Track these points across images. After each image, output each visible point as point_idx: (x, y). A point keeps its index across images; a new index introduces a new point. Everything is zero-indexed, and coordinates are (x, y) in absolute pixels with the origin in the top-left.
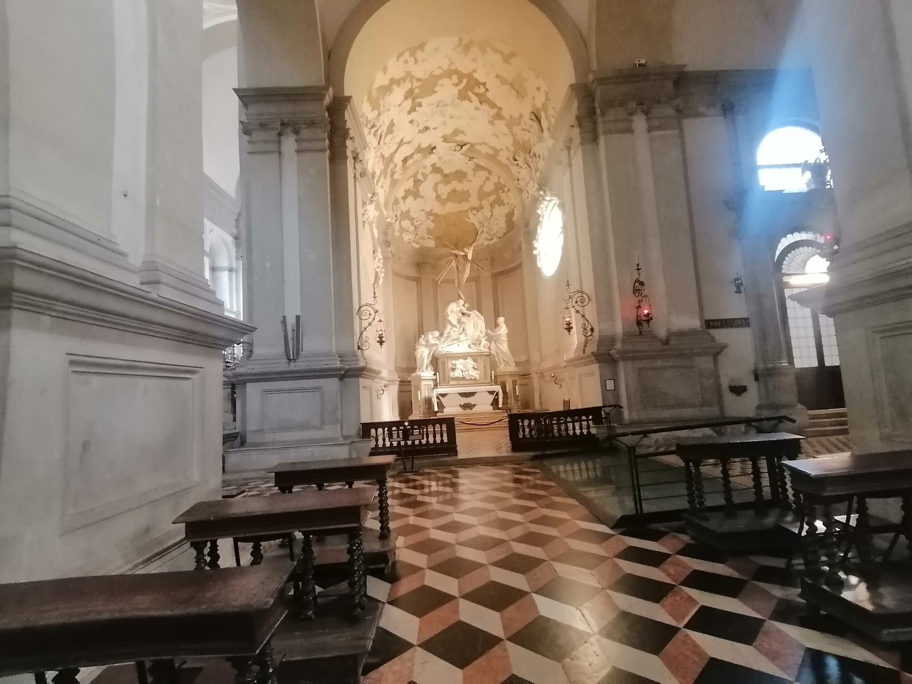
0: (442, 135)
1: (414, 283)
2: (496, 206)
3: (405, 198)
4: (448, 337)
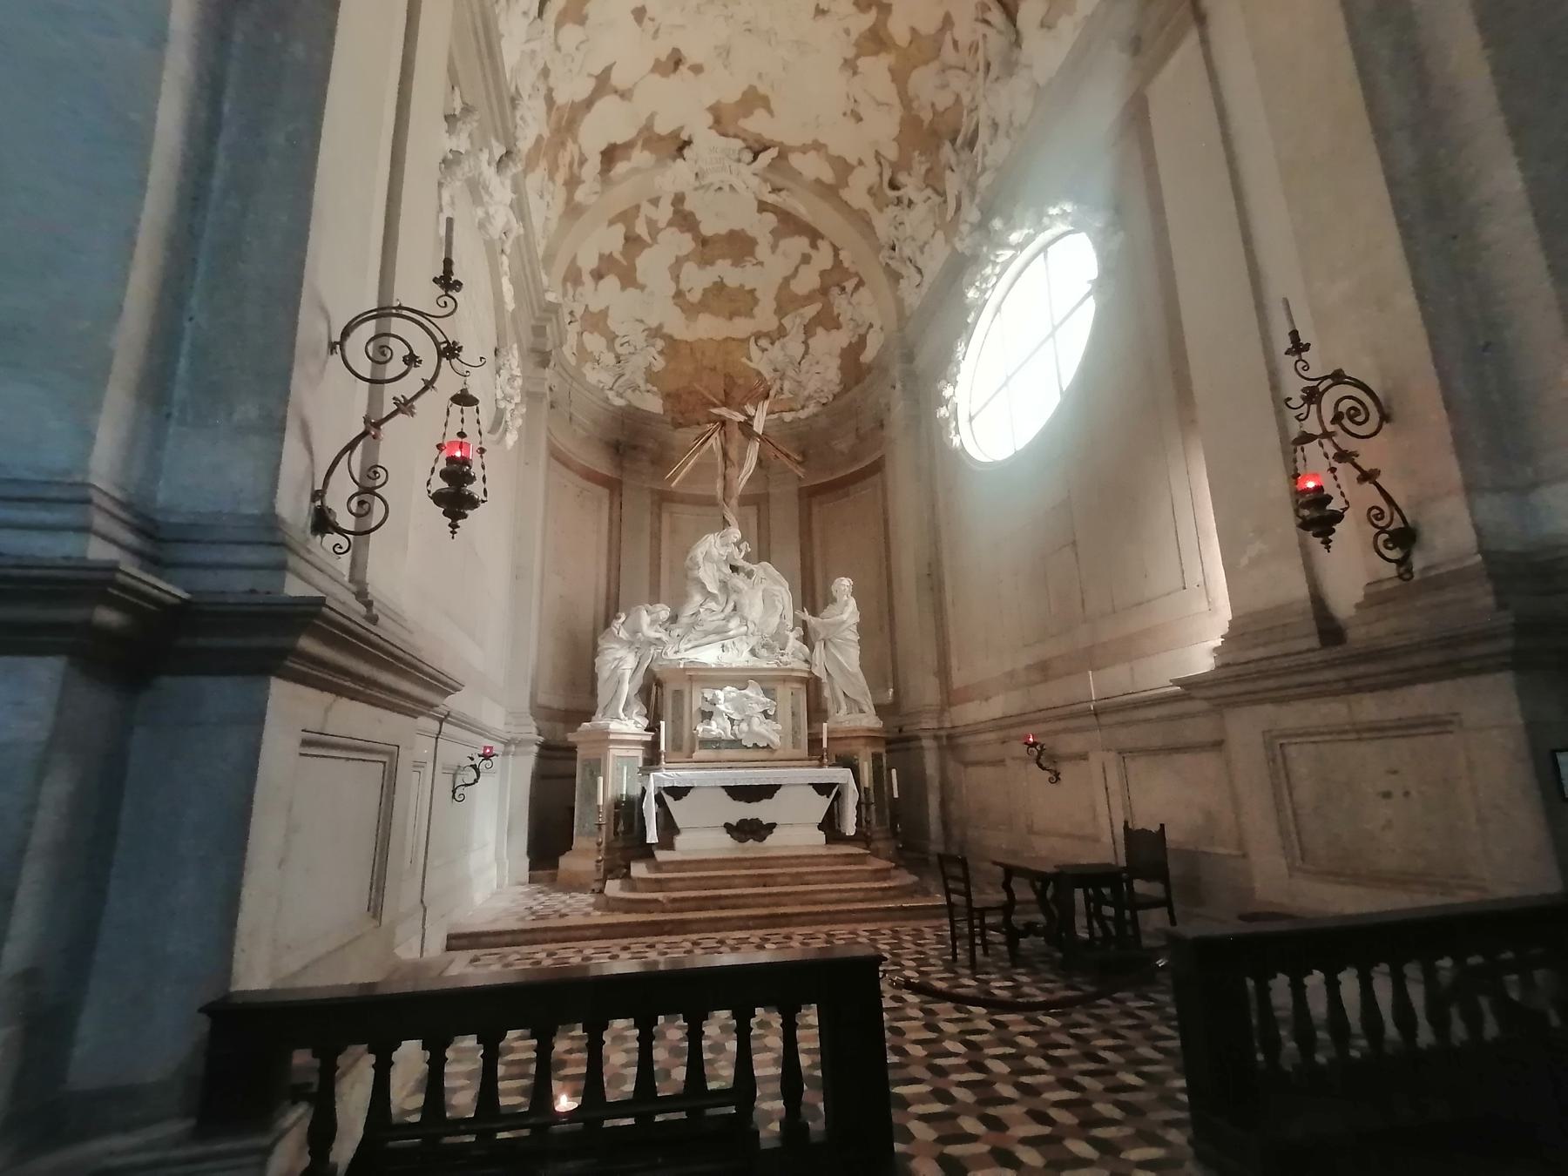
1: (603, 492)
2: (820, 331)
3: (598, 275)
4: (692, 626)
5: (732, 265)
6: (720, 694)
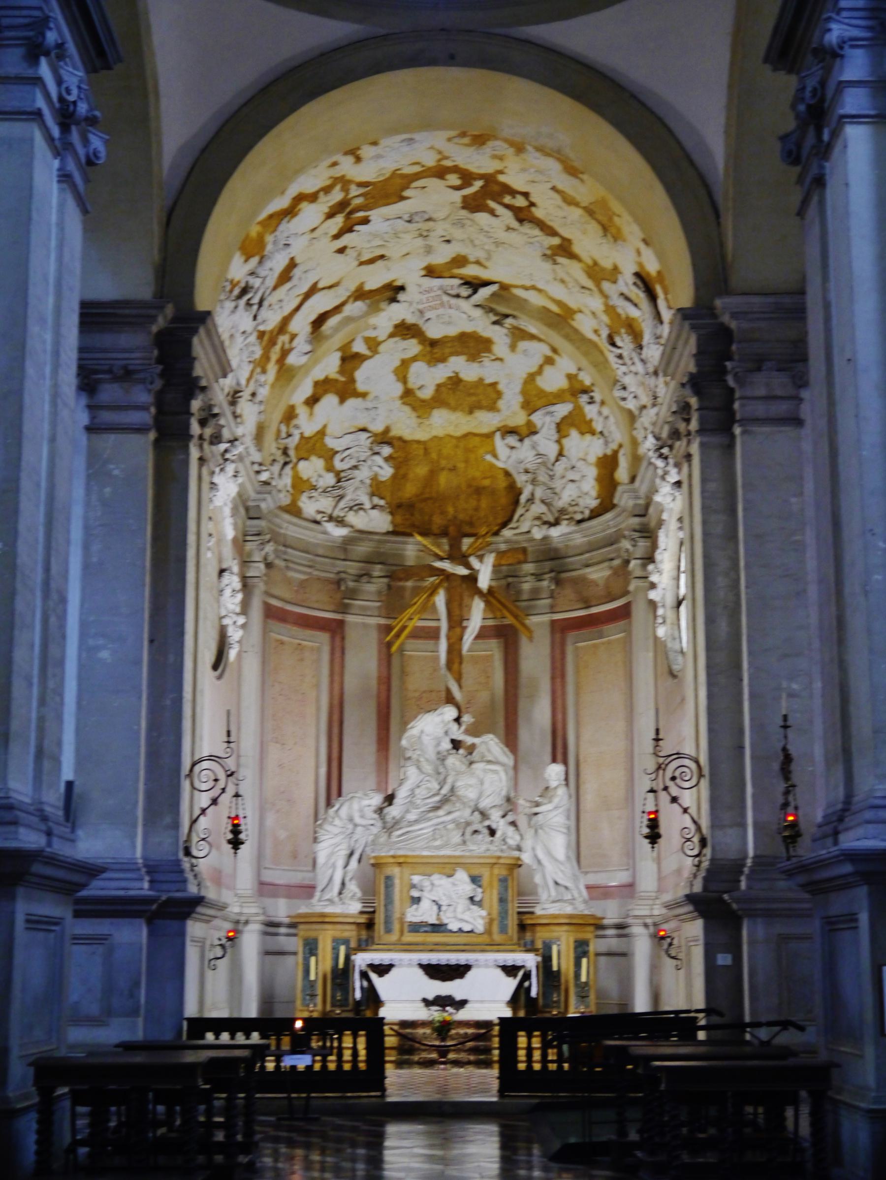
0: (424, 264)
2: (574, 433)
3: (312, 401)
5: (467, 361)
6: (426, 883)
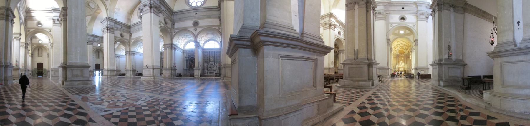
1: (396, 58)
